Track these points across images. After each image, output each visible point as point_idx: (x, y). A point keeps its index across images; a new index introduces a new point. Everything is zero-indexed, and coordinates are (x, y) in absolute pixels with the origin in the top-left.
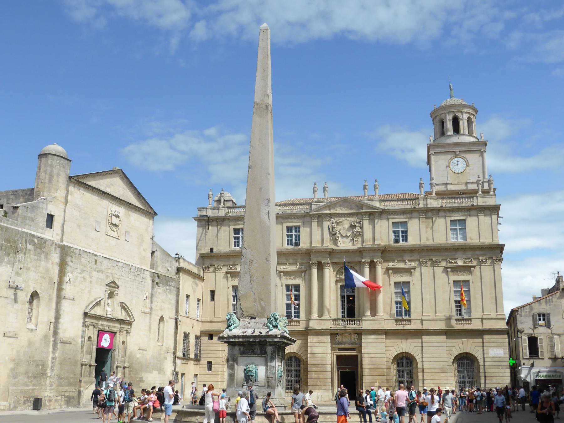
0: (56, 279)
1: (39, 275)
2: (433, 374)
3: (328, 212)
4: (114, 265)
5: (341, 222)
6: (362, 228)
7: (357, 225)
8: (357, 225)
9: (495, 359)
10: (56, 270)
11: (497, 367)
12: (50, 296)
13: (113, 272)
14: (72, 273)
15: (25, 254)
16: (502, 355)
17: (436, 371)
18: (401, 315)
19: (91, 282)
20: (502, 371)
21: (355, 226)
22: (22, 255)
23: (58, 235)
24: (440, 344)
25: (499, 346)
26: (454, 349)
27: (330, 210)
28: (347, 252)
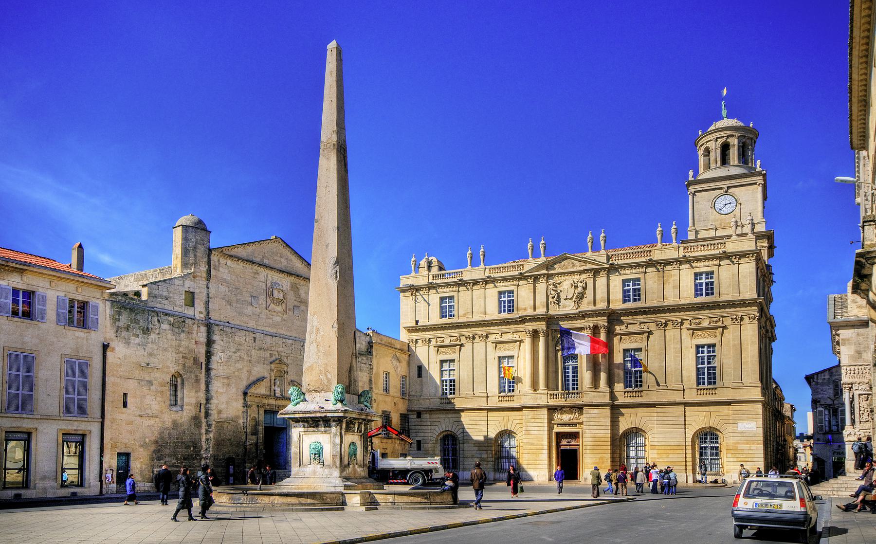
0: (203, 359)
1: (181, 355)
3: (544, 272)
4: (280, 343)
5: (560, 283)
6: (585, 288)
7: (580, 284)
8: (580, 284)
10: (202, 350)
12: (196, 376)
13: (279, 350)
14: (223, 352)
15: (159, 334)
18: (631, 386)
19: (250, 361)
21: (576, 287)
22: (157, 336)
23: (201, 313)
24: (677, 418)
27: (547, 269)
28: (568, 317)
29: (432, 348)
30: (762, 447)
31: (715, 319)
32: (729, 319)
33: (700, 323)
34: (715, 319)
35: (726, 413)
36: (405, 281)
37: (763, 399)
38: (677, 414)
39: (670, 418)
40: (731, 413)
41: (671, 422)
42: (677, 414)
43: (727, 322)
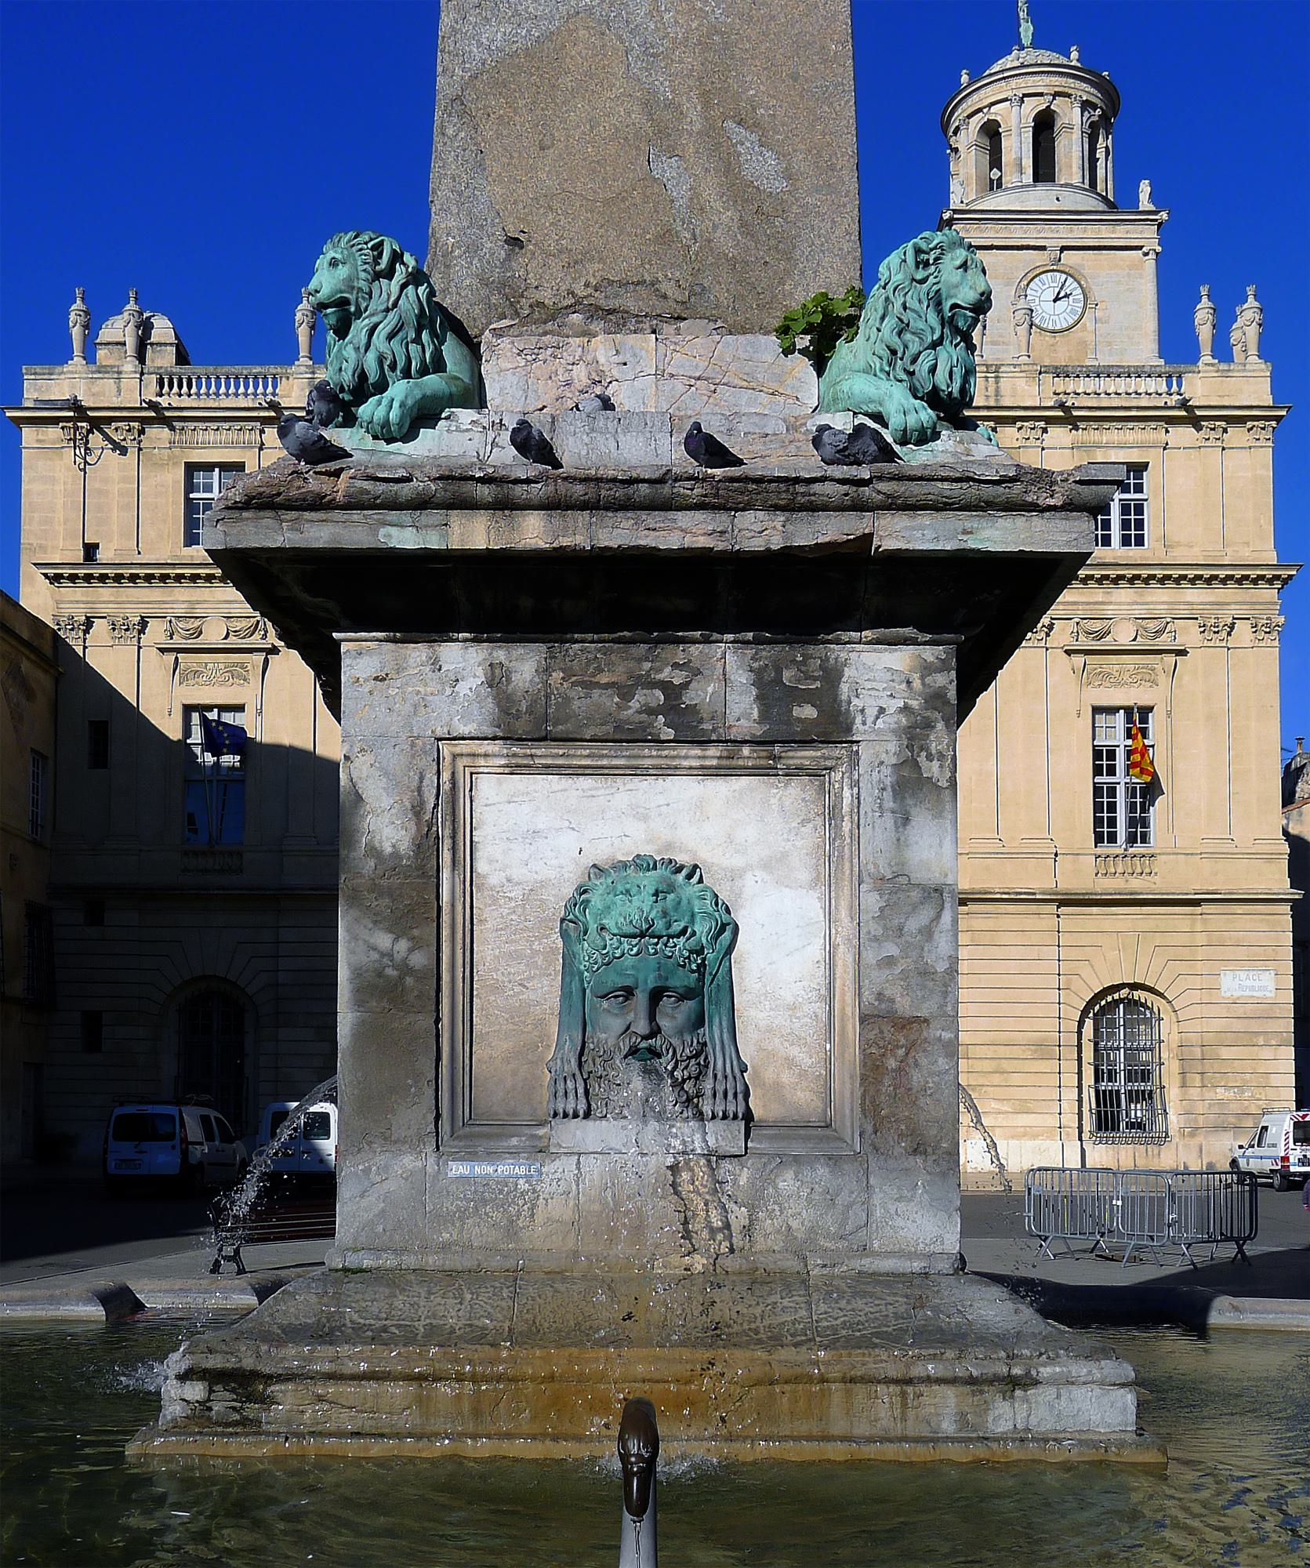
2: (1006, 1065)
9: (1240, 1011)
11: (1248, 1039)
16: (1270, 994)
17: (1016, 1052)
20: (1267, 1053)
24: (1033, 953)
25: (1255, 962)
26: (1085, 971)
29: (150, 655)
30: (1291, 1052)
31: (1152, 625)
32: (1193, 627)
33: (1101, 635)
34: (1152, 625)
35: (1183, 939)
36: (68, 382)
37: (1298, 894)
38: (1035, 938)
39: (1015, 953)
40: (1201, 939)
41: (1014, 967)
42: (1035, 938)
43: (1188, 635)
